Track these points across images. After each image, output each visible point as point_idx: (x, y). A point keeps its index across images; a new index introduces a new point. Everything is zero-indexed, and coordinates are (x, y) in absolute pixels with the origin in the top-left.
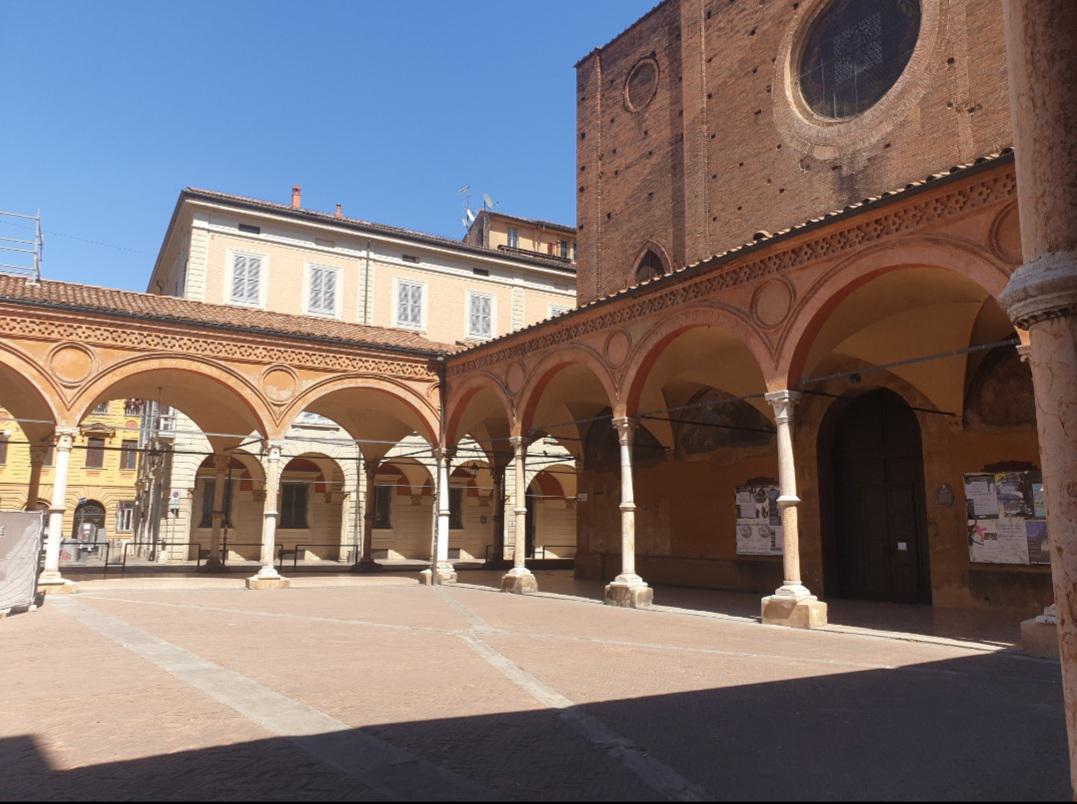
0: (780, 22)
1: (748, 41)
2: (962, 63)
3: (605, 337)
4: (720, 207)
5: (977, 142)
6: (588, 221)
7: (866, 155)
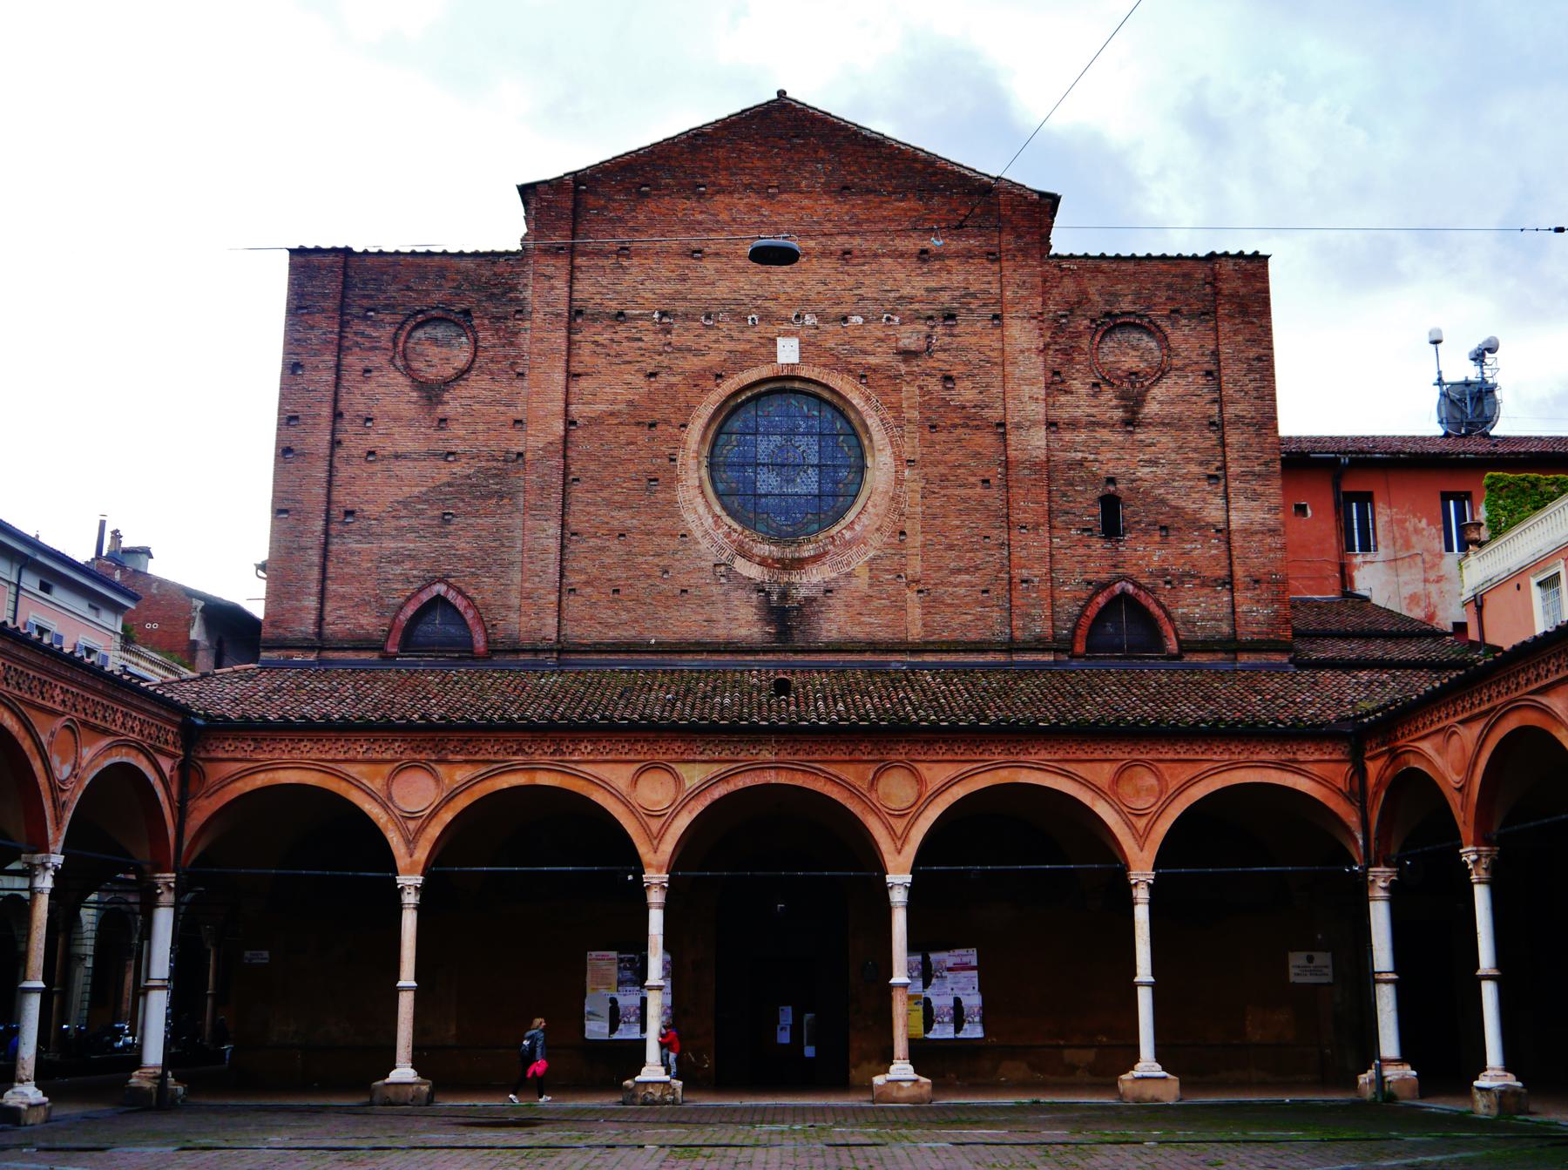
0: (695, 386)
1: (639, 380)
2: (915, 540)
3: (638, 766)
4: (583, 577)
5: (924, 625)
7: (803, 593)
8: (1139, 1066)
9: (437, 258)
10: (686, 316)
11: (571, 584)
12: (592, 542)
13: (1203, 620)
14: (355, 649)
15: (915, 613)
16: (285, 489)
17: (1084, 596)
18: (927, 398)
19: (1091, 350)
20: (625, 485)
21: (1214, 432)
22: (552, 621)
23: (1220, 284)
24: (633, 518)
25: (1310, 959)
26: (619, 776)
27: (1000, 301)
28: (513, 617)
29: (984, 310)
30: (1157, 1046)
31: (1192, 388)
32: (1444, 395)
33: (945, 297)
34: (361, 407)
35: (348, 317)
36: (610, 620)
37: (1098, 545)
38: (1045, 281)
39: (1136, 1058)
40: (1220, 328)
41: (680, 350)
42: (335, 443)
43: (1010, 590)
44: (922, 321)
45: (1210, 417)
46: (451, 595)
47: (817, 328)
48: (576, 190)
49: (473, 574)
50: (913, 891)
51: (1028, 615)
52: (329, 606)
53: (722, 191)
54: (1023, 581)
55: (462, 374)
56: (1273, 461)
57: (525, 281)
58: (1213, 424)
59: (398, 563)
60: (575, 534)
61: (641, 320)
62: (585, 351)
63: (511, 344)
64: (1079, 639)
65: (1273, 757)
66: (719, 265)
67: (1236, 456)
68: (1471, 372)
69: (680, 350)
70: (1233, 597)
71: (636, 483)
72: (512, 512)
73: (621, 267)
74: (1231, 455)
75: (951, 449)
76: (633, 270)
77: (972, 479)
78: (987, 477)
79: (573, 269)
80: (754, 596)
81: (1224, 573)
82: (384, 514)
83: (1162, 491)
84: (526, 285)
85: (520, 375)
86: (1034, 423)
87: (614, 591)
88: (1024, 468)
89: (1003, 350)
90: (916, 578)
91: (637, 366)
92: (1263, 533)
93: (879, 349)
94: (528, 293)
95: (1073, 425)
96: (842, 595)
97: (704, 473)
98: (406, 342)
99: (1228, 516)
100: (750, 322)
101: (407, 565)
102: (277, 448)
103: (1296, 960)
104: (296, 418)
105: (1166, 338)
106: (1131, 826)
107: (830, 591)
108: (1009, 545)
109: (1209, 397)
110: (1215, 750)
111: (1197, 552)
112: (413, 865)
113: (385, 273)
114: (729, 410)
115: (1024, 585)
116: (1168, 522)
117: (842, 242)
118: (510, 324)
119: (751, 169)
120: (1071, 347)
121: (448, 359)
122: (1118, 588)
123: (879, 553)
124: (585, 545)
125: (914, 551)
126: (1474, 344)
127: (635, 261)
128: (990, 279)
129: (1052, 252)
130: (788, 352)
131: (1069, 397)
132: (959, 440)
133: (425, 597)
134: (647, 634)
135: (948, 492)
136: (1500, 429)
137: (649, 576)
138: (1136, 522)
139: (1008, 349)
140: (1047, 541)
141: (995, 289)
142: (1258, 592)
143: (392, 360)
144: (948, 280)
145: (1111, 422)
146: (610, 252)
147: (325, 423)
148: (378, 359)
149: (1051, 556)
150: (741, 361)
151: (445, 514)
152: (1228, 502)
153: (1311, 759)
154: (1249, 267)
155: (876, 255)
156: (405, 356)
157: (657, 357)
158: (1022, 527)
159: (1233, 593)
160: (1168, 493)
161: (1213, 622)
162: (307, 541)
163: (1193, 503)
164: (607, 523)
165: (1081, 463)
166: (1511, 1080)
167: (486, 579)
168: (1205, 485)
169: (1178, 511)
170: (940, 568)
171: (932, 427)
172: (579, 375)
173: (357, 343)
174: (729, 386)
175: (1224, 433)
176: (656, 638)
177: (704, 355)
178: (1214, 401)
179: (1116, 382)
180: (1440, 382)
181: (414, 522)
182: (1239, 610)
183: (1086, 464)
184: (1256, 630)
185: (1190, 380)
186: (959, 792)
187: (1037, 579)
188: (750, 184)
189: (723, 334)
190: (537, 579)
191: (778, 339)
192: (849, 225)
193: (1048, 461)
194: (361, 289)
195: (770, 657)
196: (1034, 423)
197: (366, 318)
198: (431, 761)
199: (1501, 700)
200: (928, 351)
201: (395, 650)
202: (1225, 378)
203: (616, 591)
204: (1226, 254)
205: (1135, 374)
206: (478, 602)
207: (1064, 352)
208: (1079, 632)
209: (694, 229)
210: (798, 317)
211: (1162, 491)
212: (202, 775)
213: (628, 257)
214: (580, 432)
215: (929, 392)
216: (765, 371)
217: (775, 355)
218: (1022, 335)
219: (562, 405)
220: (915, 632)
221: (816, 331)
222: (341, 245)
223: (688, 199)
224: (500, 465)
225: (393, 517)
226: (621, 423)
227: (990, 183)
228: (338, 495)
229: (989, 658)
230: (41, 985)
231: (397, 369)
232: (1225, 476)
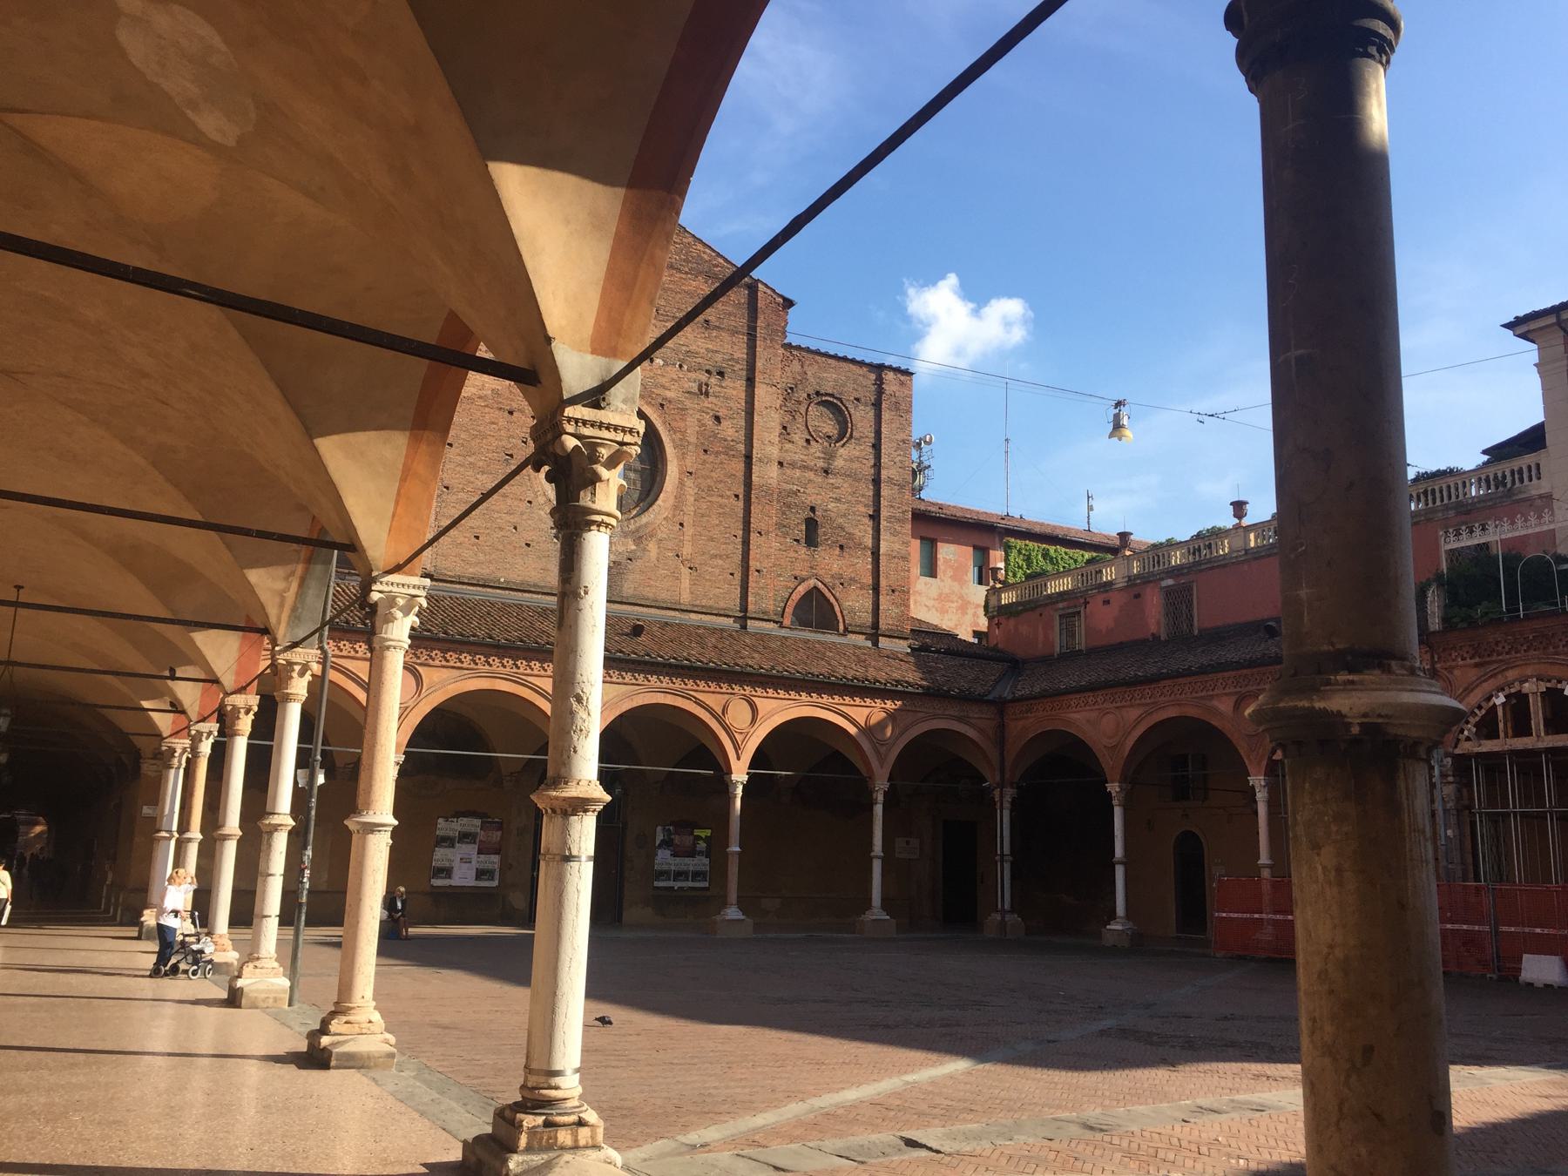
2: (689, 531)
8: (875, 911)
15: (686, 582)
17: (793, 586)
25: (908, 843)
29: (740, 373)
30: (883, 900)
33: (719, 357)
37: (803, 550)
39: (868, 904)
51: (759, 594)
54: (758, 571)
60: (447, 488)
65: (956, 714)
77: (728, 493)
86: (770, 461)
90: (689, 557)
95: (793, 465)
96: (639, 563)
106: (878, 752)
111: (860, 565)
116: (842, 541)
120: (795, 411)
122: (812, 582)
123: (665, 536)
124: (455, 497)
131: (790, 445)
132: (722, 463)
134: (499, 574)
135: (714, 499)
137: (501, 529)
138: (825, 539)
144: (721, 345)
153: (976, 716)
164: (472, 483)
166: (1130, 925)
169: (851, 536)
170: (704, 554)
176: (504, 577)
179: (820, 440)
184: (891, 622)
186: (778, 720)
196: (770, 461)
198: (417, 664)
199: (1162, 698)
202: (883, 451)
203: (477, 537)
205: (829, 437)
215: (704, 425)
220: (686, 598)
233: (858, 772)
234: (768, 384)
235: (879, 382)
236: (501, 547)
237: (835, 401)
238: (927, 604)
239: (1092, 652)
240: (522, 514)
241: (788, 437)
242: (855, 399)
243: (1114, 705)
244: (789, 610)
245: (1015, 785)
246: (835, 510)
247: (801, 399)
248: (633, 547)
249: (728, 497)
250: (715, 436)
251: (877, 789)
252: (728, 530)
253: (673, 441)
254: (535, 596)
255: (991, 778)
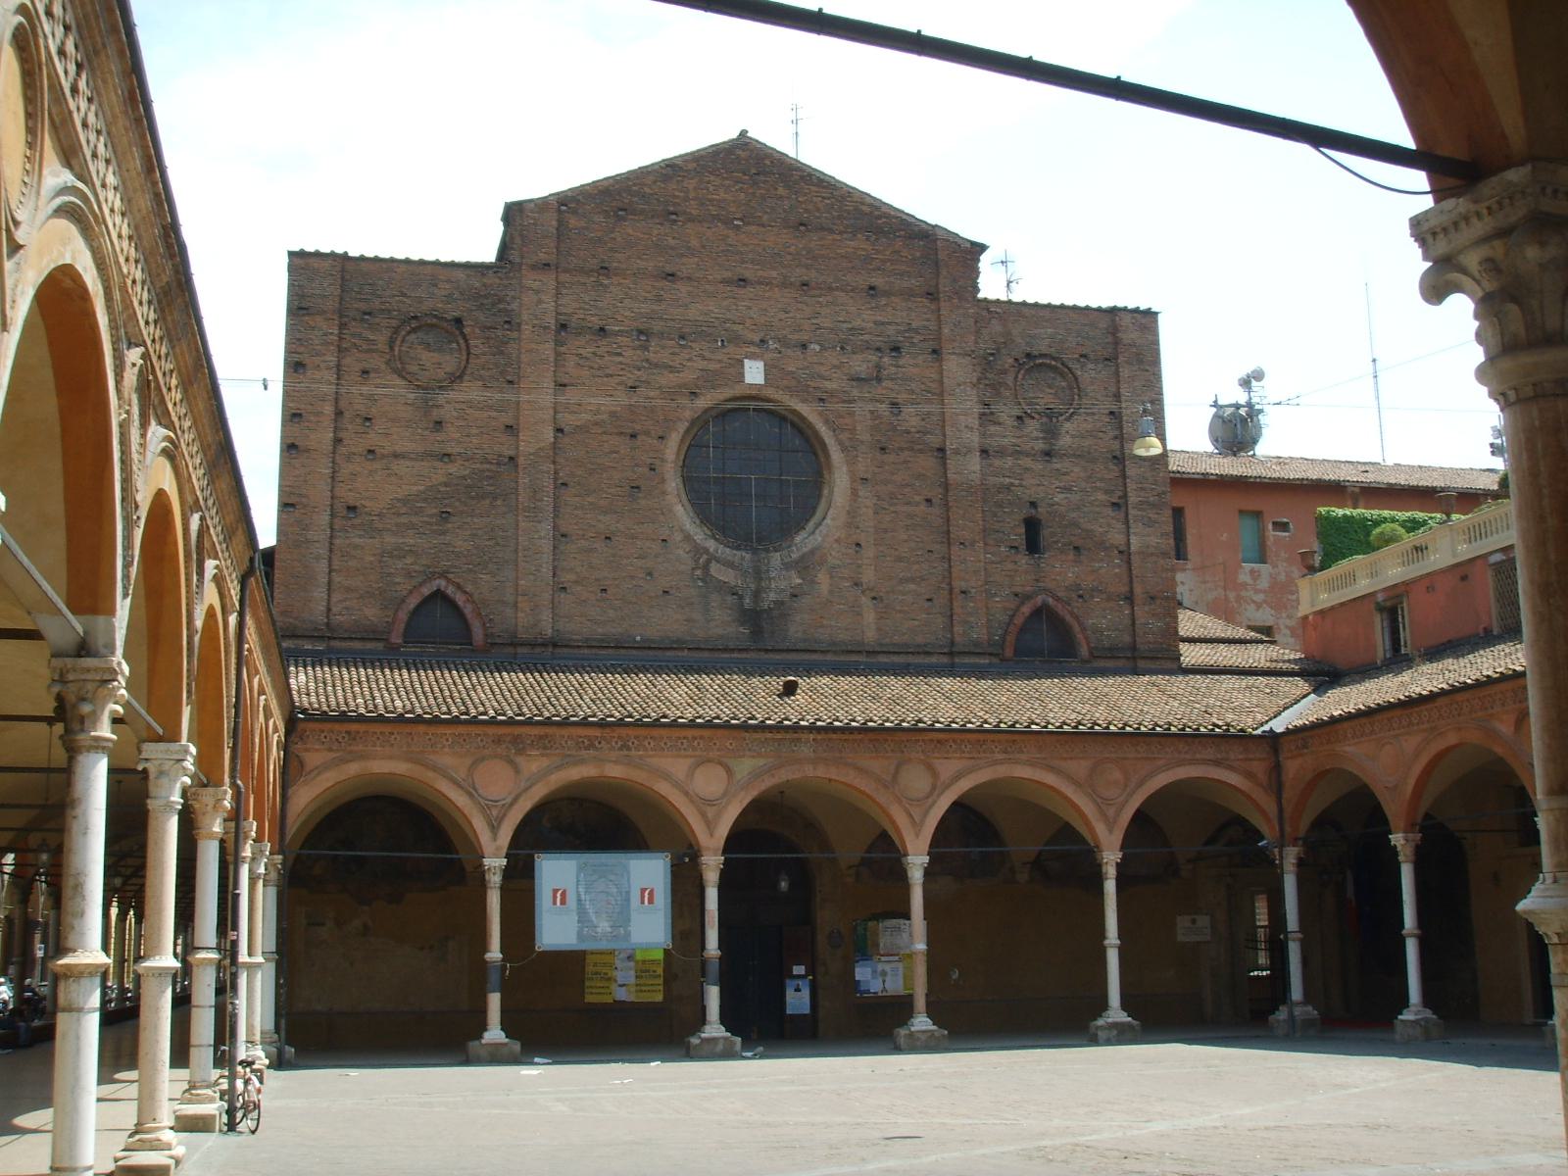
2: (869, 552)
3: (689, 761)
4: (571, 577)
5: (879, 629)
6: (303, 500)
7: (772, 596)
8: (1110, 1012)
9: (429, 267)
10: (661, 335)
11: (563, 583)
12: (583, 543)
13: (1109, 630)
14: (362, 639)
15: (870, 617)
16: (288, 483)
18: (877, 422)
19: (1015, 386)
20: (609, 491)
21: (1116, 465)
22: (546, 616)
23: (1119, 335)
24: (618, 522)
25: (1194, 921)
26: (678, 767)
27: (938, 339)
28: (509, 612)
31: (1099, 424)
32: (1216, 416)
33: (891, 330)
34: (356, 407)
35: (346, 319)
36: (599, 618)
37: (1024, 560)
38: (976, 322)
40: (1121, 374)
41: (656, 366)
42: (338, 441)
43: (951, 600)
44: (872, 352)
45: (1113, 451)
46: (450, 591)
47: (780, 353)
48: (559, 211)
49: (471, 570)
50: (928, 873)
52: (334, 599)
53: (691, 220)
54: (963, 592)
55: (456, 378)
56: (1164, 493)
57: (513, 293)
58: (1115, 457)
59: (400, 558)
60: (562, 536)
61: (621, 336)
62: (571, 363)
63: (502, 353)
64: (1007, 644)
65: (1211, 757)
66: (690, 289)
67: (1134, 487)
68: (1241, 397)
69: (656, 366)
70: (1133, 611)
71: (619, 489)
72: (505, 514)
73: (601, 285)
74: (1131, 486)
75: (899, 470)
76: (612, 288)
77: (917, 498)
78: (929, 497)
79: (559, 284)
80: (729, 598)
81: (1124, 589)
82: (384, 511)
83: (1074, 515)
84: (514, 298)
85: (510, 382)
86: (969, 451)
87: (602, 590)
88: (962, 490)
89: (941, 383)
91: (617, 380)
92: (1158, 556)
93: (834, 375)
94: (515, 306)
95: (1001, 452)
97: (679, 480)
98: (401, 346)
99: (1129, 540)
100: (720, 344)
101: (409, 560)
102: (281, 443)
103: (1183, 922)
104: (300, 415)
105: (1076, 379)
107: (796, 596)
108: (950, 560)
109: (1112, 434)
110: (1167, 749)
112: (498, 849)
113: (381, 279)
114: (700, 423)
115: (963, 595)
117: (798, 274)
118: (499, 333)
119: (719, 201)
121: (440, 364)
122: (1039, 600)
123: (838, 562)
125: (866, 561)
126: (1243, 374)
127: (615, 280)
128: (928, 316)
129: (981, 295)
130: (754, 373)
132: (905, 462)
133: (426, 591)
136: (1262, 449)
137: (632, 577)
139: (945, 380)
140: (982, 557)
141: (933, 325)
142: (1152, 607)
143: (387, 363)
145: (1033, 452)
146: (592, 271)
147: (327, 422)
148: (376, 362)
149: (985, 569)
150: (711, 379)
151: (443, 512)
152: (1128, 528)
154: (1143, 321)
155: (831, 289)
156: (400, 359)
157: (636, 372)
158: (961, 543)
159: (1133, 607)
160: (1080, 517)
161: (1117, 632)
162: (310, 535)
163: (1100, 526)
165: (1008, 488)
167: (482, 576)
168: (1109, 511)
171: (883, 449)
172: (565, 385)
173: (355, 344)
174: (703, 403)
175: (1124, 466)
177: (678, 372)
178: (1116, 438)
180: (1215, 404)
181: (414, 519)
182: (1137, 622)
183: (1012, 488)
185: (1096, 418)
186: (964, 785)
187: (974, 590)
188: (717, 215)
189: (695, 353)
190: (532, 577)
191: (746, 361)
192: (807, 259)
193: (982, 484)
194: (358, 293)
195: (744, 655)
197: (362, 320)
200: (879, 380)
201: (400, 641)
202: (1125, 418)
204: (1125, 309)
206: (476, 597)
207: (996, 388)
208: (1008, 638)
209: (667, 253)
210: (762, 341)
211: (1074, 515)
212: (302, 764)
213: (608, 277)
214: (567, 440)
215: (879, 417)
216: (738, 391)
217: (742, 375)
218: (957, 369)
219: (552, 412)
220: (870, 635)
221: (779, 355)
222: (340, 250)
223: (661, 224)
224: (493, 467)
225: (394, 514)
226: (605, 433)
227: (927, 231)
228: (338, 492)
229: (934, 660)
230: (172, 963)
231: (395, 371)
232: (1126, 502)
233: (1084, 841)
234: (960, 354)
235: (1114, 331)
236: (634, 600)
237: (1053, 363)
238: (1254, 598)
239: (1401, 662)
240: (656, 556)
241: (991, 418)
242: (1081, 356)
243: (1392, 733)
244: (1011, 638)
245: (1300, 842)
246: (1064, 502)
247: (1007, 366)
248: (799, 581)
249: (917, 504)
250: (894, 429)
251: (1105, 861)
252: (921, 545)
253: (840, 443)
254: (680, 654)
255: (1269, 832)
